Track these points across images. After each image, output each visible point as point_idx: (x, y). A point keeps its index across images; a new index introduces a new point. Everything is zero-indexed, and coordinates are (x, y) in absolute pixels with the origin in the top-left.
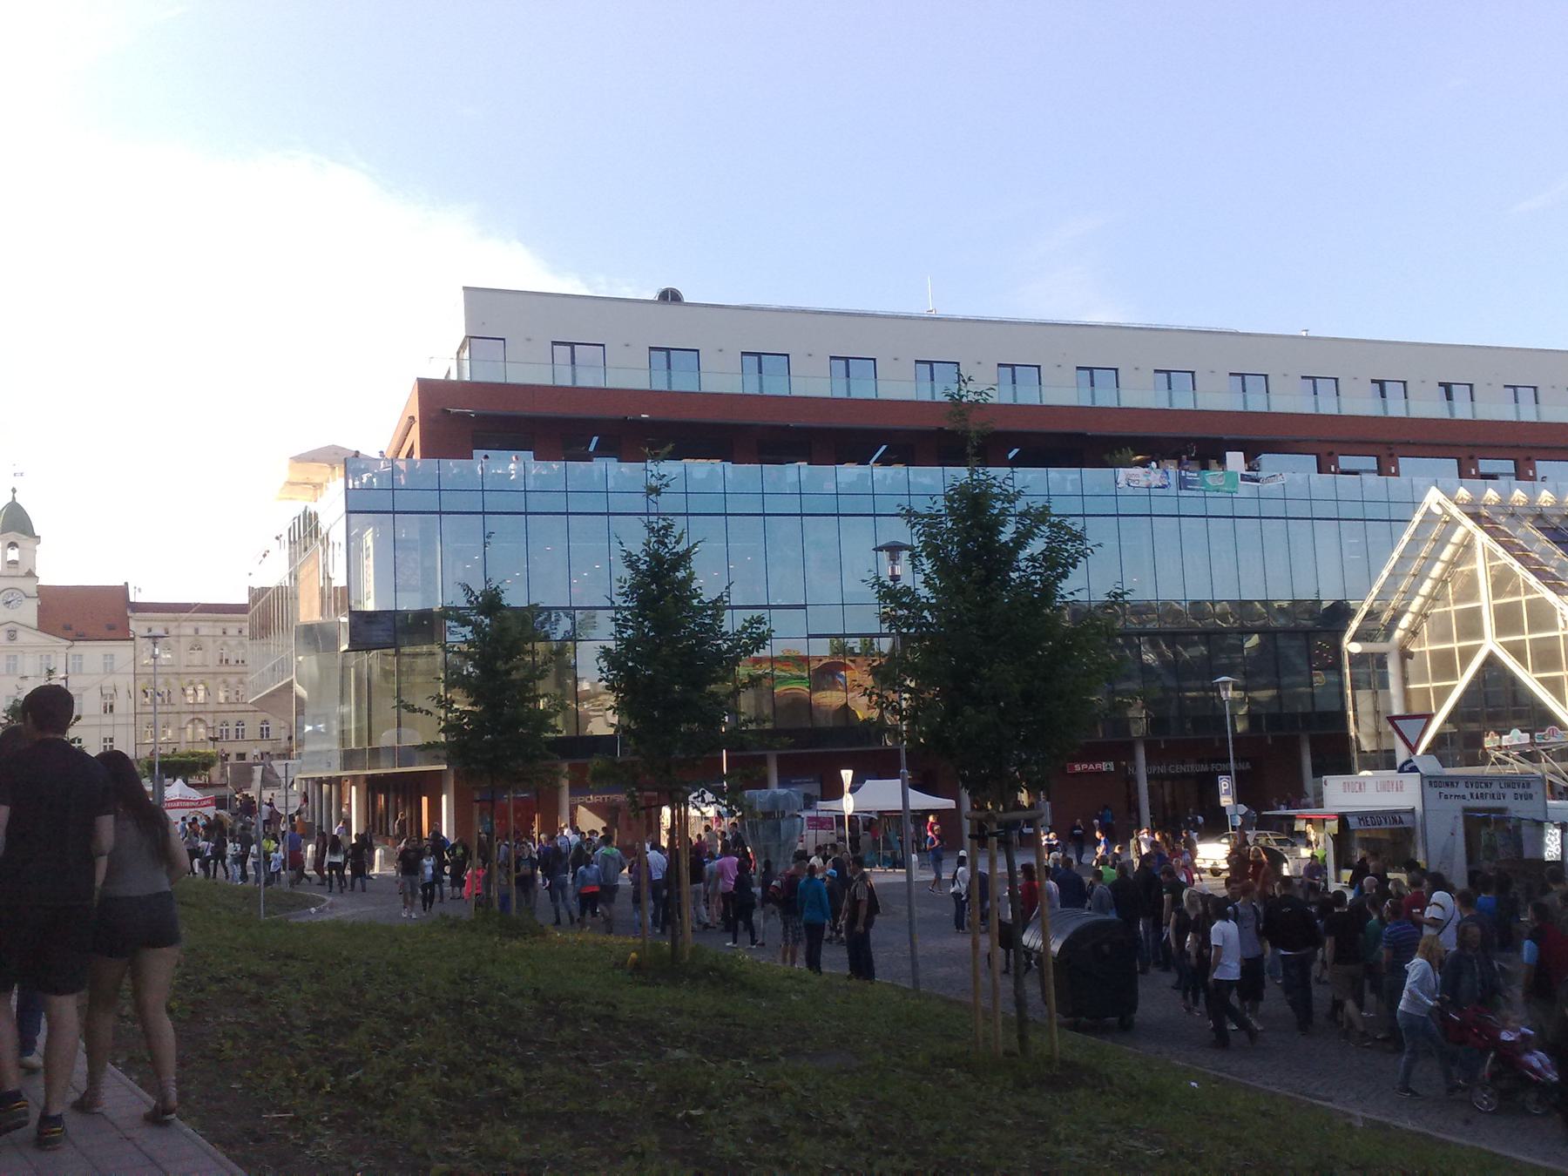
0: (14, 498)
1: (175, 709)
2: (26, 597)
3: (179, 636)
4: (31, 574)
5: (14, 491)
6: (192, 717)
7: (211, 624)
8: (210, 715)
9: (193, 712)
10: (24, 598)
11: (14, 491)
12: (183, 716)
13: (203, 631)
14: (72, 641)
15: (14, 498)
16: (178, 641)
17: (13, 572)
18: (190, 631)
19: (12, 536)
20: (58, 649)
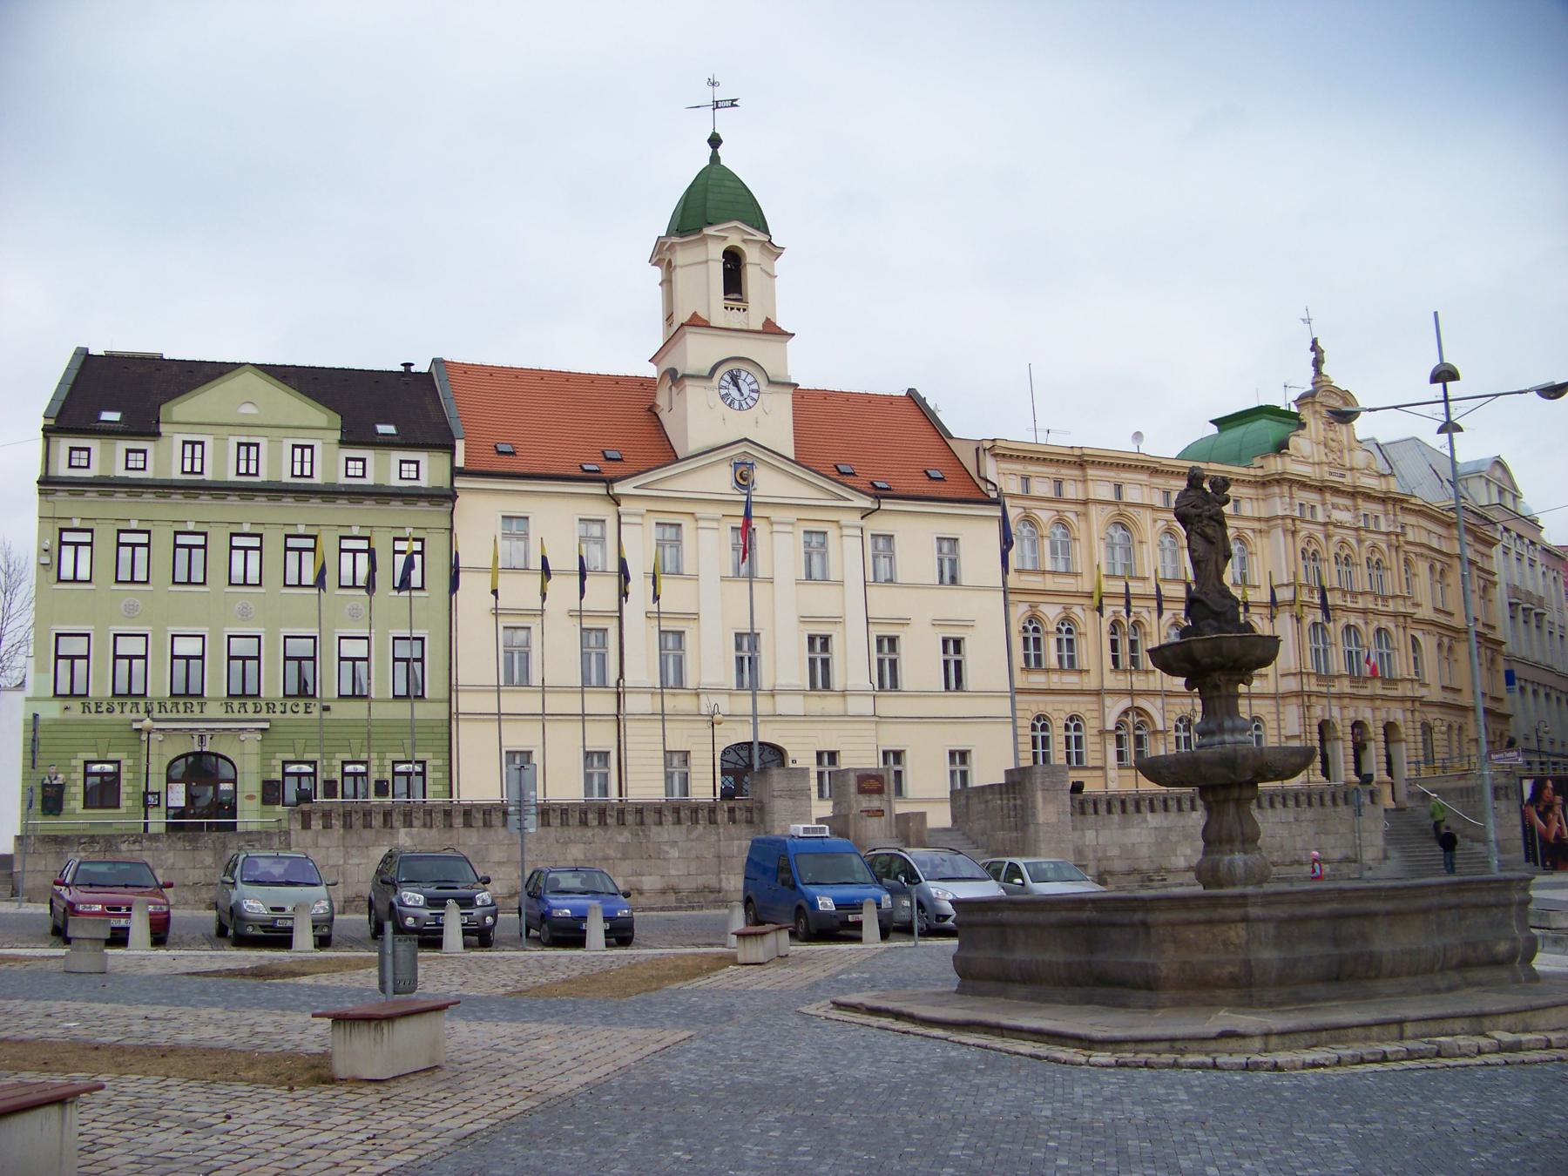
0: (715, 159)
1: (1091, 682)
2: (771, 383)
3: (1085, 502)
4: (771, 329)
5: (715, 141)
6: (1125, 703)
7: (1143, 477)
8: (1158, 702)
9: (1131, 693)
10: (764, 387)
11: (715, 141)
12: (1108, 701)
13: (1131, 494)
14: (878, 498)
15: (715, 159)
16: (1086, 515)
17: (735, 320)
18: (1106, 492)
19: (733, 234)
20: (845, 518)
